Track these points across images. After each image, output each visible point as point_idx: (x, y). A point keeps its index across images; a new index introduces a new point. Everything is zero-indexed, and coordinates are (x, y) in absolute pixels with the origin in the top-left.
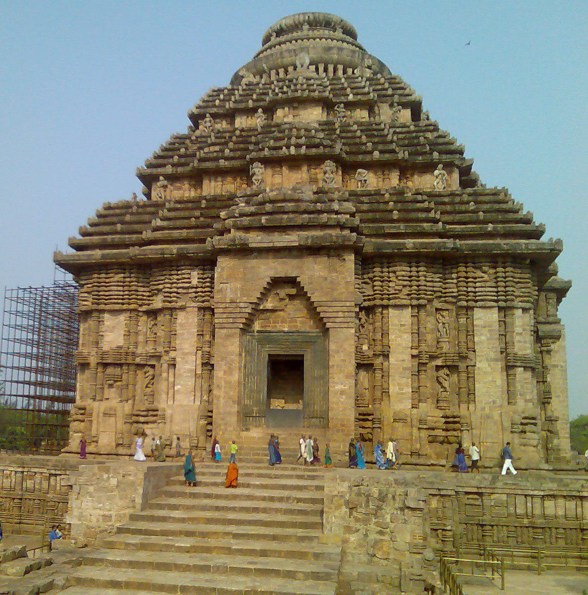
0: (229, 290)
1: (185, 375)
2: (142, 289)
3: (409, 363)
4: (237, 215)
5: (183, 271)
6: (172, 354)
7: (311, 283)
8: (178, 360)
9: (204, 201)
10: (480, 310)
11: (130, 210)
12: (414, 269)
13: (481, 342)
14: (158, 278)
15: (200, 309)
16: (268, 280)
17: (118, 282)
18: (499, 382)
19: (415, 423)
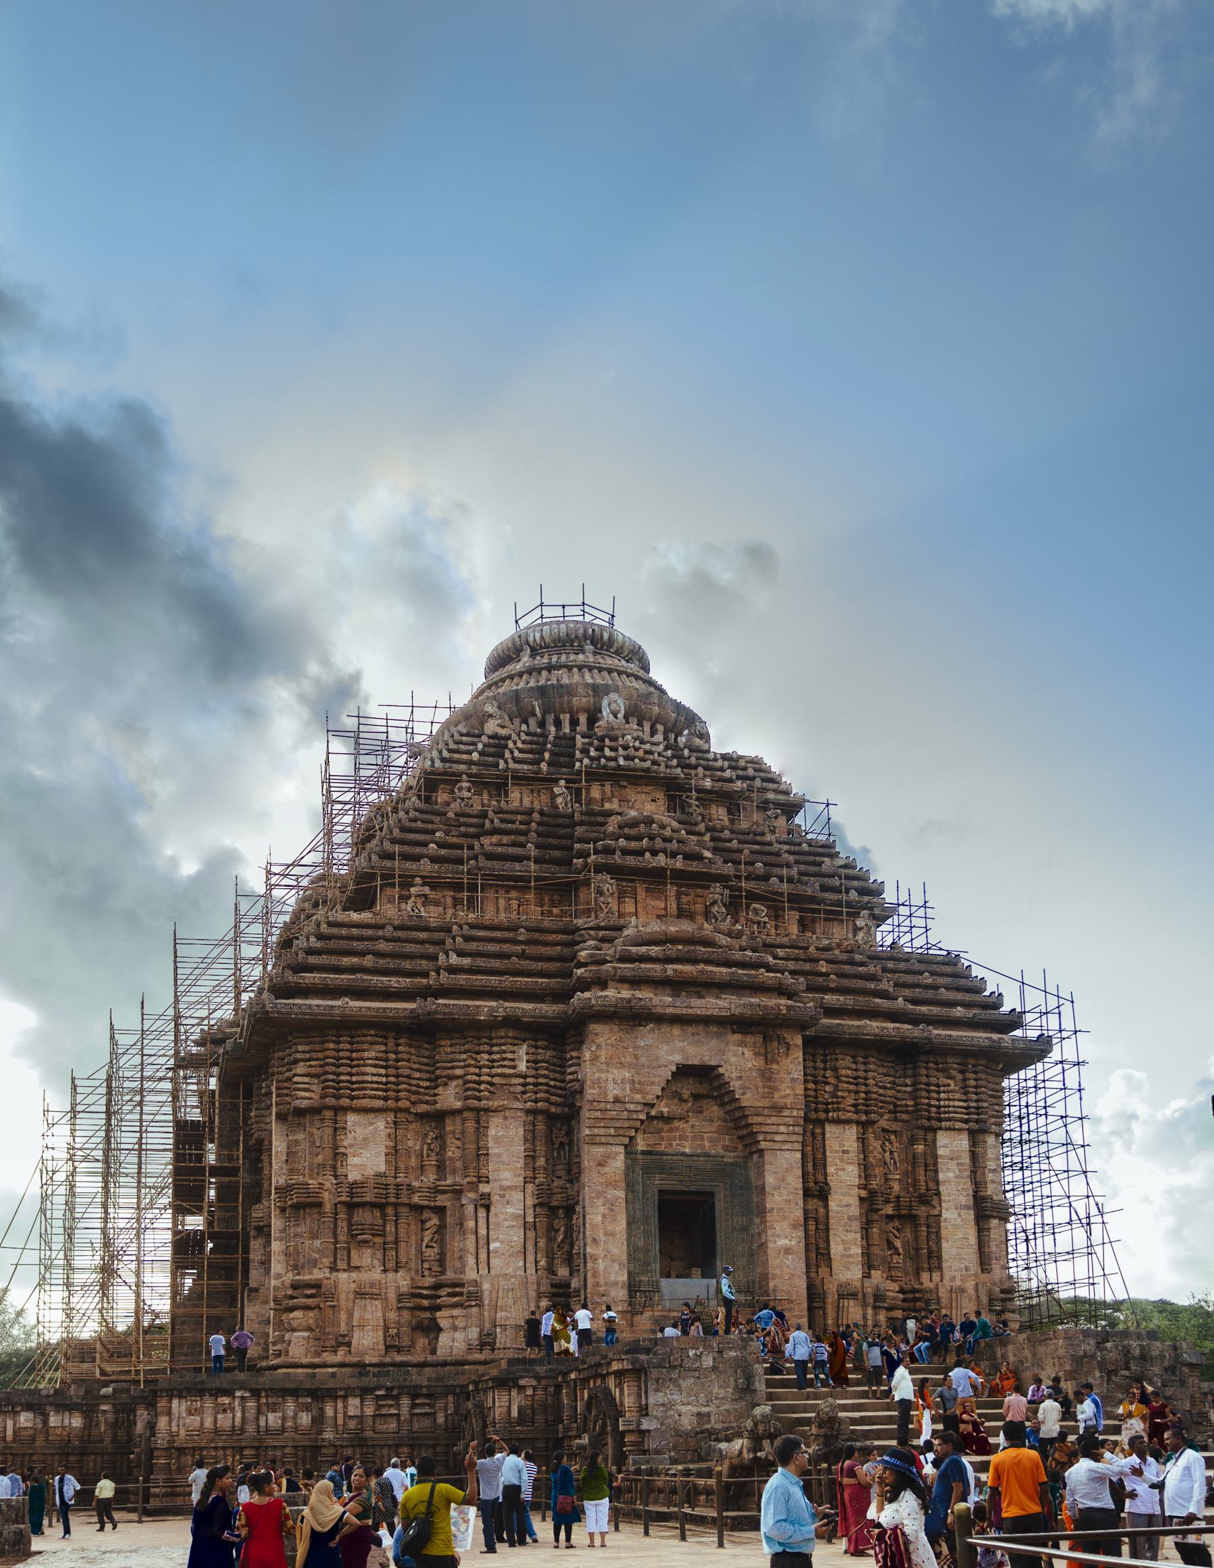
0: (611, 1086)
1: (506, 1224)
2: (417, 1075)
3: (855, 1211)
4: (608, 958)
5: (503, 1048)
6: (484, 1188)
7: (740, 1078)
8: (495, 1198)
9: (522, 930)
10: (946, 1134)
11: (381, 933)
12: (862, 1067)
13: (949, 1182)
14: (451, 1056)
15: (528, 1112)
16: (674, 1068)
17: (376, 1059)
18: (973, 1239)
19: (871, 1301)
